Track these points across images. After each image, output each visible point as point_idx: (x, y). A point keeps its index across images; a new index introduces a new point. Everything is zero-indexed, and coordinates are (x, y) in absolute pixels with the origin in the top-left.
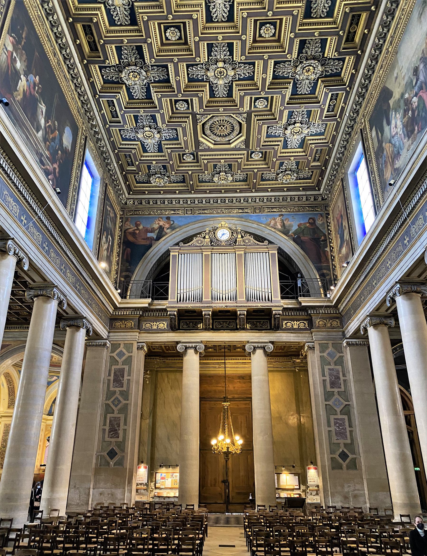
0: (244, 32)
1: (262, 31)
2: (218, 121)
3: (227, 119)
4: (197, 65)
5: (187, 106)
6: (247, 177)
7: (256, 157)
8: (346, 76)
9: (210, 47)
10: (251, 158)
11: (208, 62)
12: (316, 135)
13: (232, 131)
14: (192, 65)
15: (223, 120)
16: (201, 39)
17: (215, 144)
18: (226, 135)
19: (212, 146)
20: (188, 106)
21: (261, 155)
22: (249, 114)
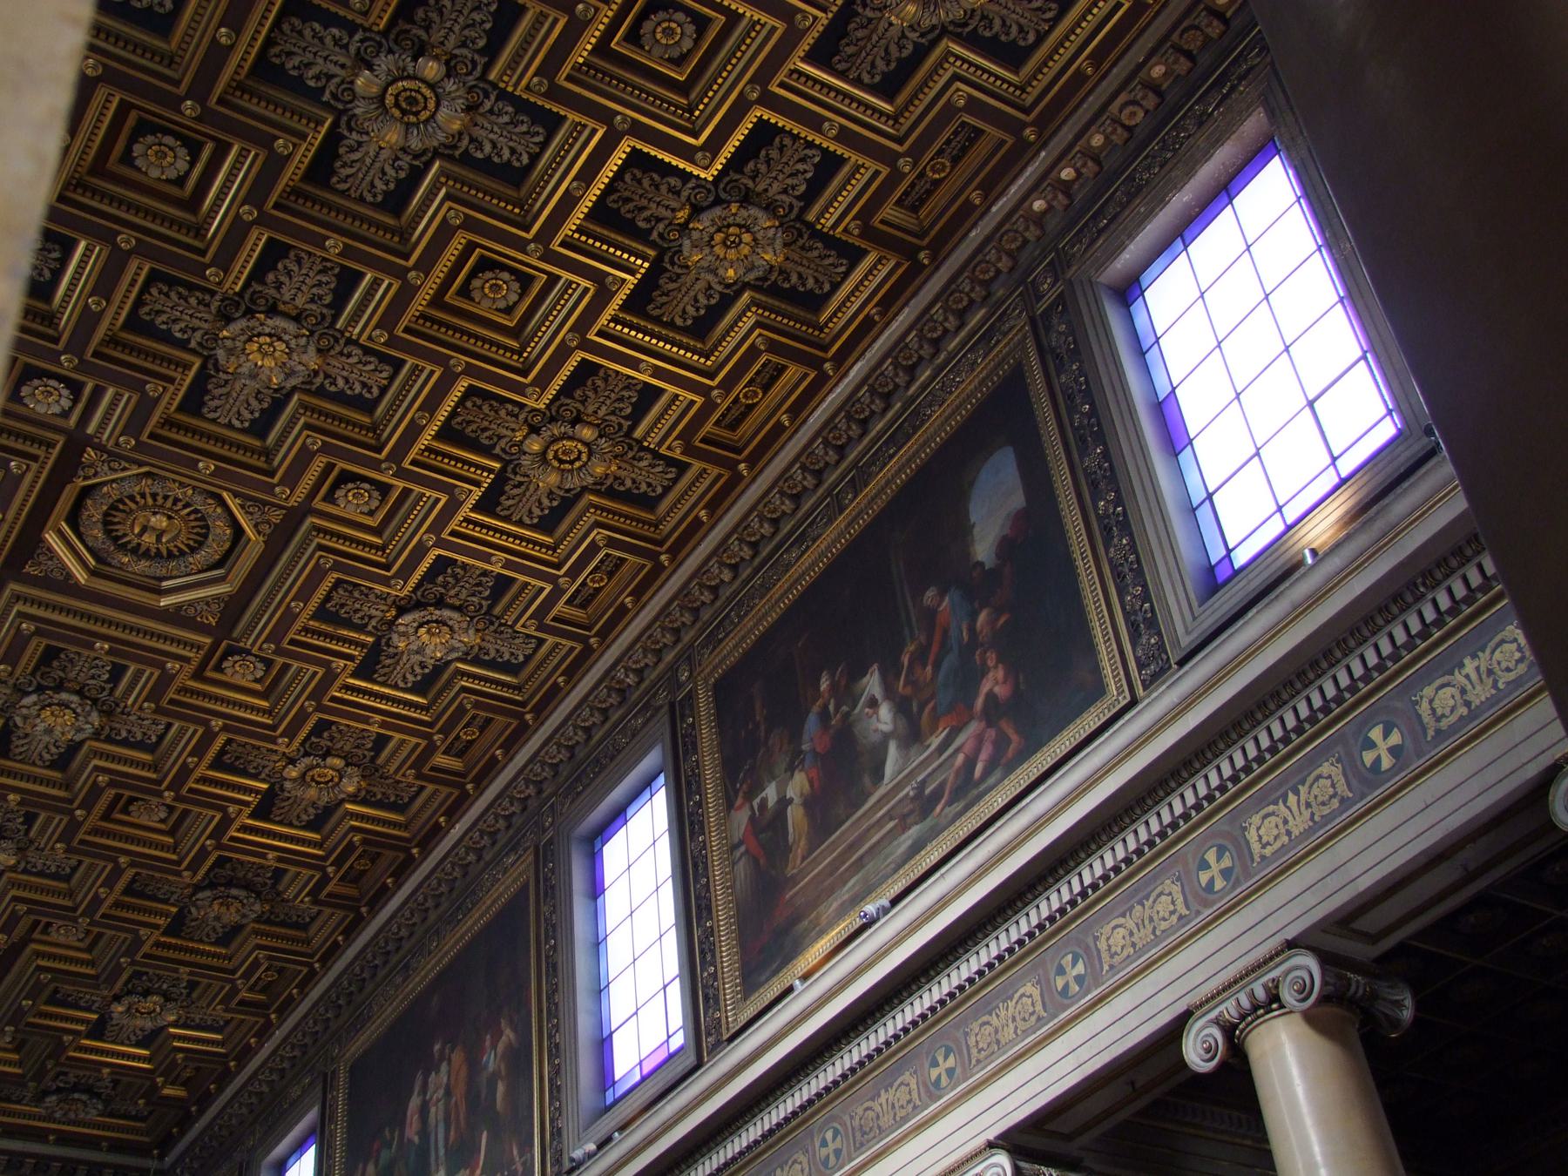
0: (426, 265)
1: (476, 283)
2: (154, 496)
3: (198, 498)
4: (191, 287)
5: (66, 403)
6: (161, 738)
7: (242, 672)
8: (671, 515)
9: (273, 254)
10: (218, 668)
11: (241, 294)
12: (492, 665)
13: (193, 550)
14: (173, 282)
15: (176, 500)
16: (263, 221)
17: (93, 573)
18: (158, 554)
19: (81, 576)
20: (71, 409)
21: (259, 674)
22: (294, 518)
